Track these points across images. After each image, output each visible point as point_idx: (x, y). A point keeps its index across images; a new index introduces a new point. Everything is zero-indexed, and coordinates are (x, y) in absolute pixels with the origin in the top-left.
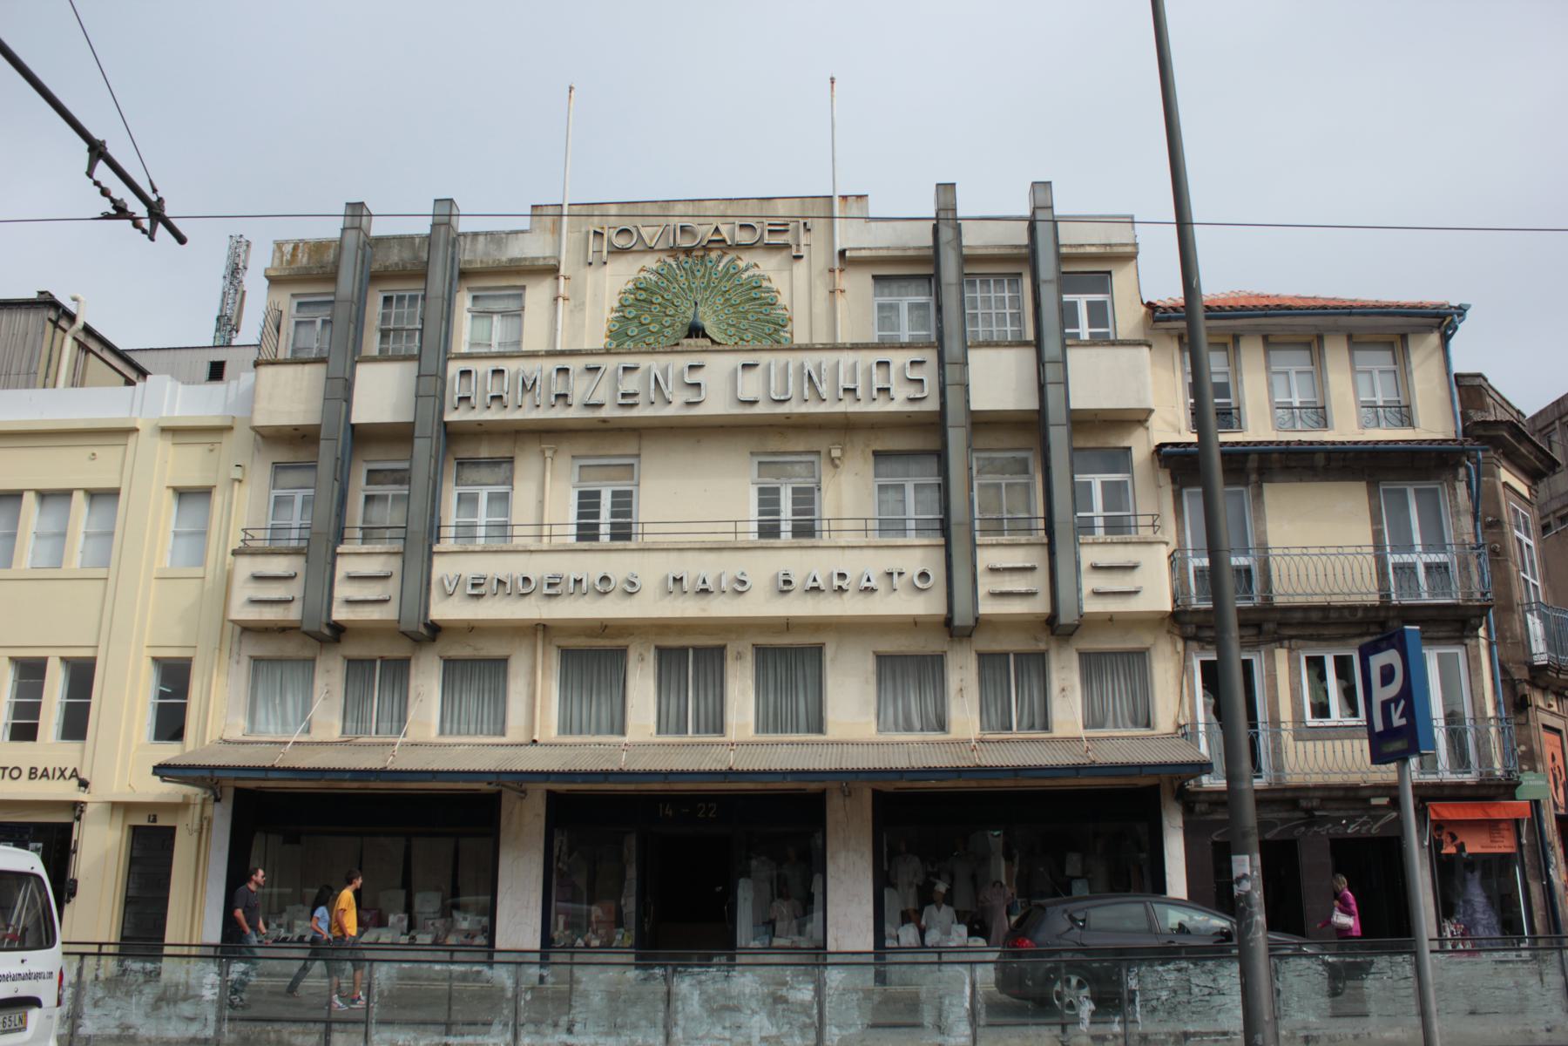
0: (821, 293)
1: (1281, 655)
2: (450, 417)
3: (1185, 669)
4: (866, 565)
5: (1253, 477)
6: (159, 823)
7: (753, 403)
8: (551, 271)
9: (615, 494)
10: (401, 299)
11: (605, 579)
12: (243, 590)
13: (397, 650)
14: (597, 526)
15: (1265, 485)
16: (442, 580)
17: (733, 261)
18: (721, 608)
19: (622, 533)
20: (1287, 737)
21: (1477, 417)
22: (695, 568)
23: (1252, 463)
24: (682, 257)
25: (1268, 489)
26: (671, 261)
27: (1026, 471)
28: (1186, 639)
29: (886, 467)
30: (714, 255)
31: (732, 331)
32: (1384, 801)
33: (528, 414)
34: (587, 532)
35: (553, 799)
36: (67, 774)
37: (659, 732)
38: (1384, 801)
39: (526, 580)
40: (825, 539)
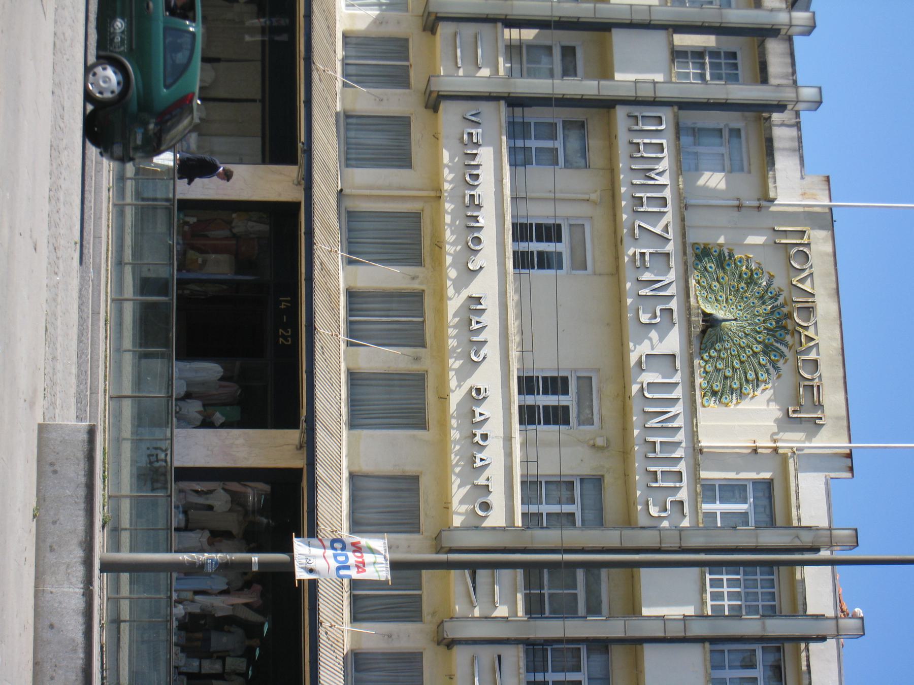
11: (478, 240)
13: (416, 78)
17: (782, 355)
30: (788, 338)
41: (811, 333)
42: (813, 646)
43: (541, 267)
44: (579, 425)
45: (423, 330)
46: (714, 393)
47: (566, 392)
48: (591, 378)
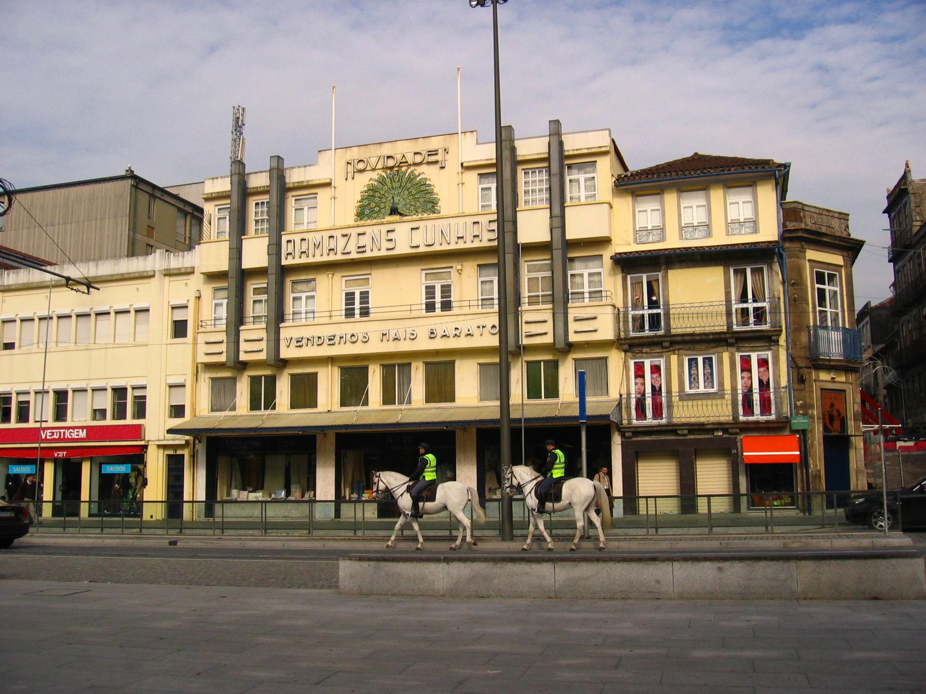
1: (674, 358)
2: (284, 262)
3: (626, 367)
4: (470, 324)
7: (418, 247)
8: (328, 185)
9: (361, 293)
12: (202, 349)
14: (354, 309)
17: (412, 172)
18: (405, 346)
19: (365, 312)
20: (675, 399)
21: (791, 226)
22: (392, 328)
24: (389, 171)
25: (671, 273)
26: (383, 174)
28: (625, 351)
29: (485, 272)
30: (404, 169)
33: (318, 259)
34: (350, 313)
35: (338, 436)
37: (427, 401)
39: (319, 338)
40: (455, 311)
42: (566, 148)
43: (368, 303)
46: (433, 207)
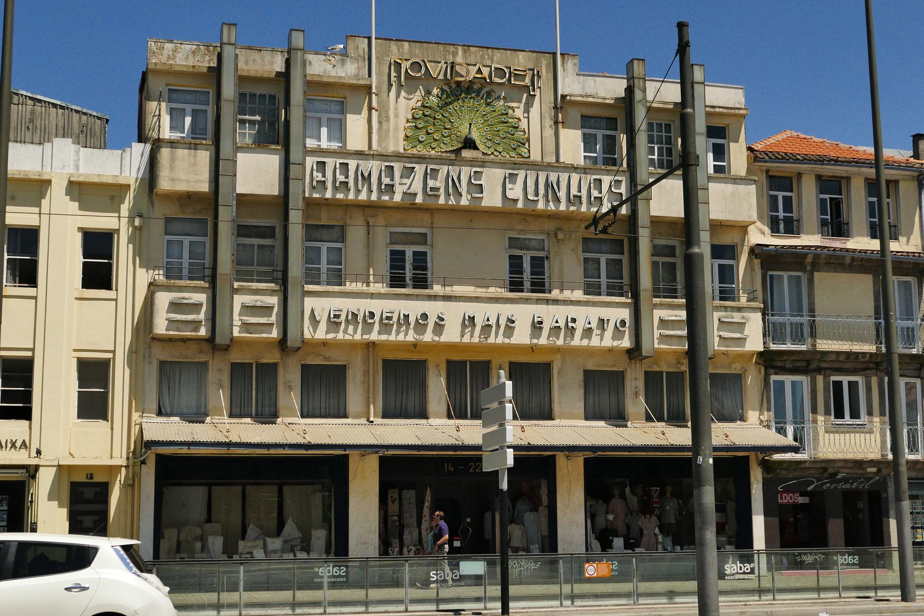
0: (549, 122)
5: (809, 268)
6: (95, 480)
7: (516, 201)
10: (253, 96)
15: (816, 275)
16: (312, 311)
23: (809, 259)
27: (673, 255)
31: (489, 144)
32: (874, 470)
36: (18, 444)
38: (874, 470)
41: (476, 68)
44: (544, 250)
45: (455, 362)
47: (521, 257)
48: (510, 238)
